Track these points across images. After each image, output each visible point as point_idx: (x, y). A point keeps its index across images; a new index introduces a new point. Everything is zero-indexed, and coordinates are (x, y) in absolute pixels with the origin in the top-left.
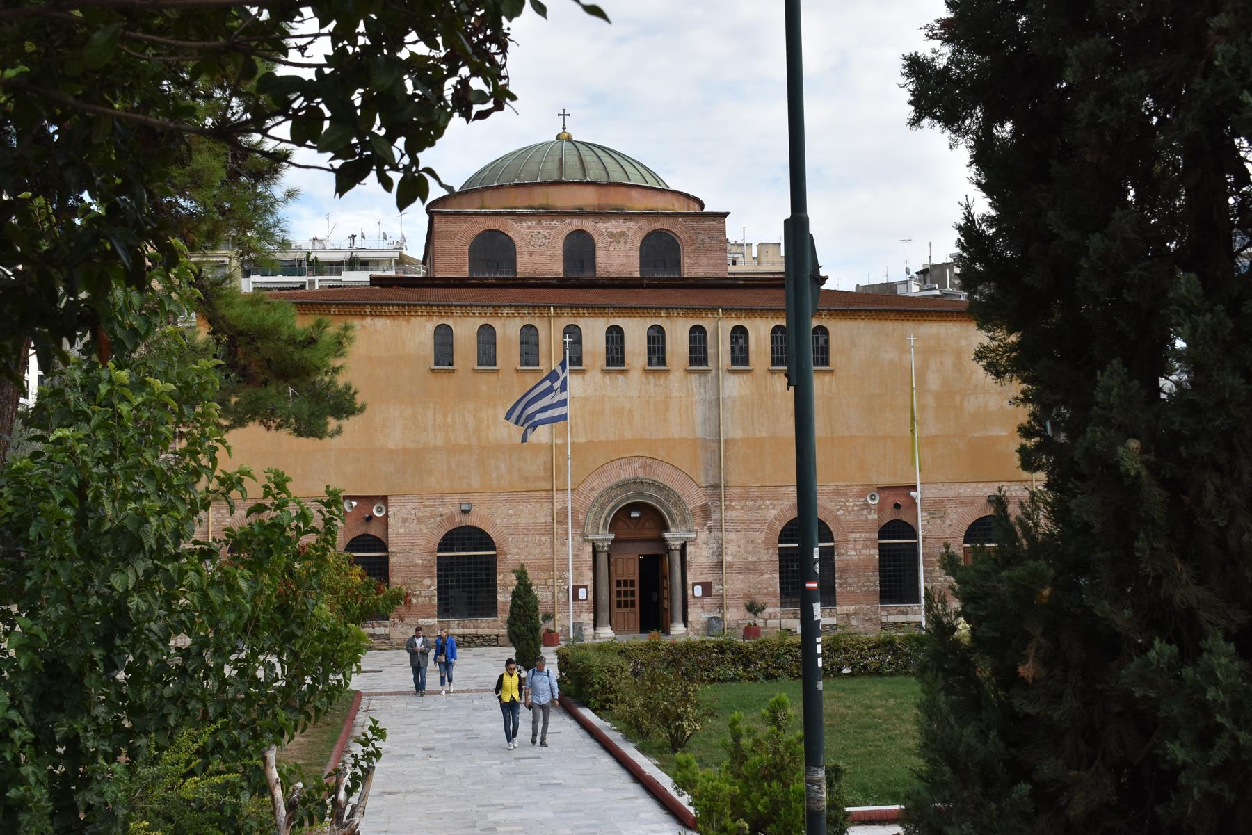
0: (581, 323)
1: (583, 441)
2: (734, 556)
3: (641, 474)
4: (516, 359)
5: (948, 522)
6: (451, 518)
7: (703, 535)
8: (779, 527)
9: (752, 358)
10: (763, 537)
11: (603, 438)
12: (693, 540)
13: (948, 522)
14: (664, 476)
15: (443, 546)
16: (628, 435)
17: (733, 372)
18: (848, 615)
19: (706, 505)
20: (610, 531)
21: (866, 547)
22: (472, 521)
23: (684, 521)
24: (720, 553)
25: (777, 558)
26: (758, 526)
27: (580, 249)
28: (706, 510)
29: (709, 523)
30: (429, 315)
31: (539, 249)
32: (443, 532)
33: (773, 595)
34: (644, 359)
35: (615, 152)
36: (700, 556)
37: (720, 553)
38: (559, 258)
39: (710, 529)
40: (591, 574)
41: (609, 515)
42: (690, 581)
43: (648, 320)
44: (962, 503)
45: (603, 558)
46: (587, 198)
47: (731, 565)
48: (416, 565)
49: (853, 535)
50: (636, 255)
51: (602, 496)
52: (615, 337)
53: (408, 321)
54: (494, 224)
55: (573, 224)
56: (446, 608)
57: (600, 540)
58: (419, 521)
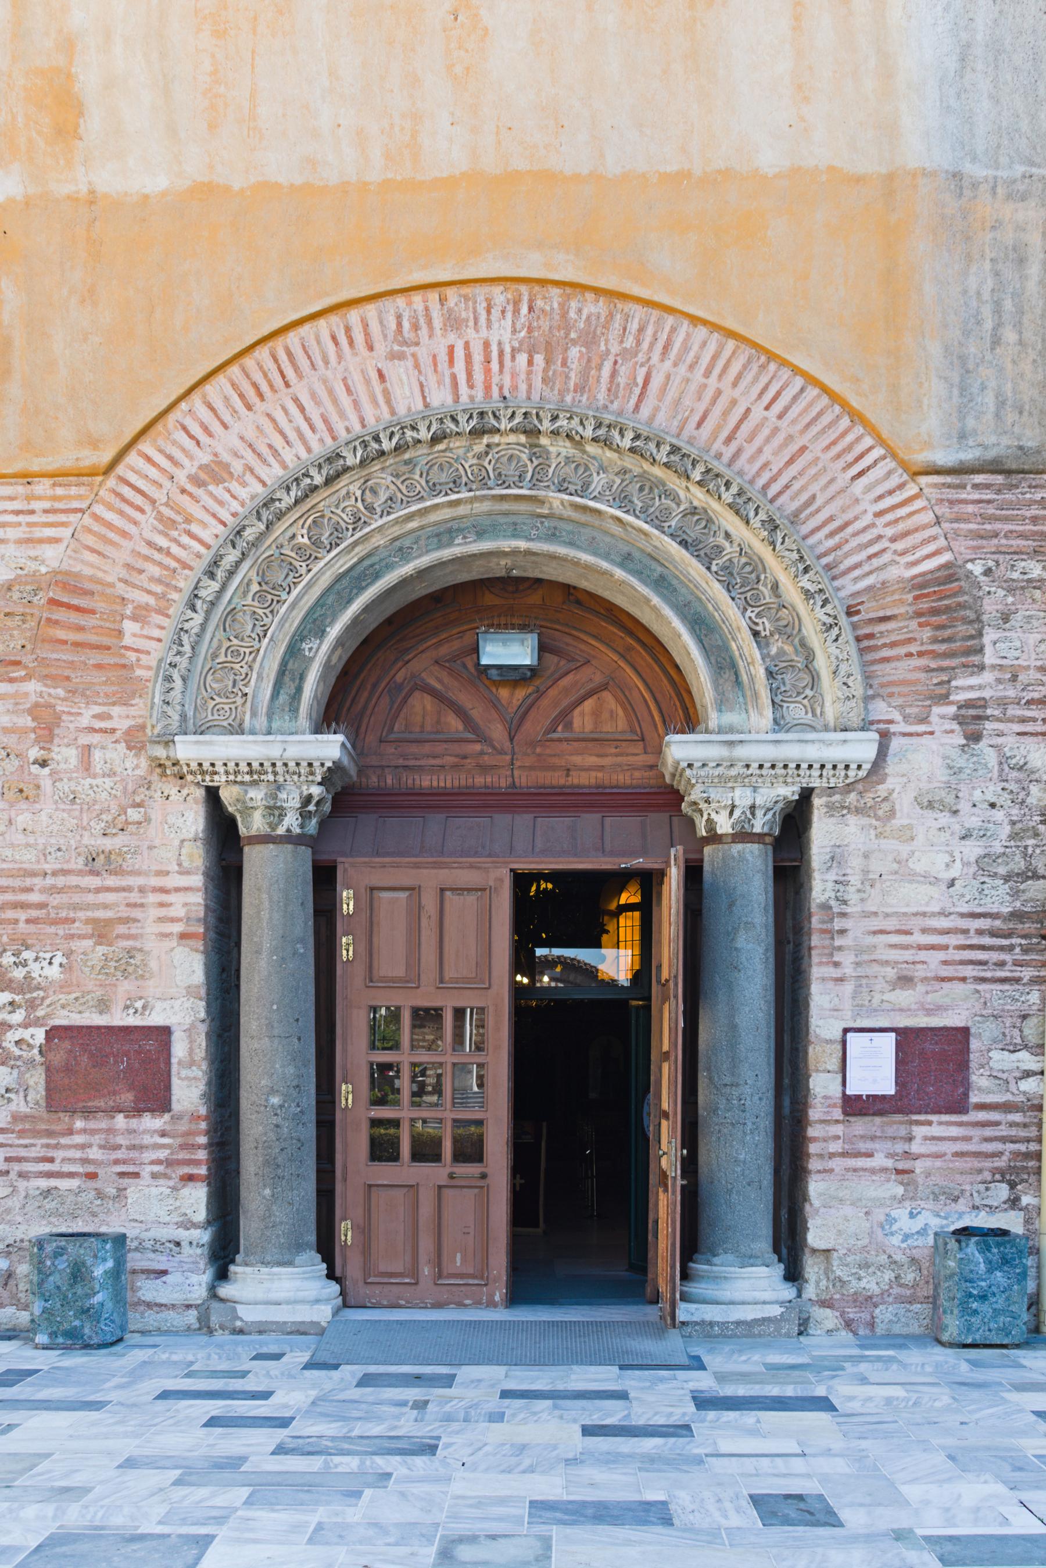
1: (157, 183)
7: (927, 756)
11: (279, 166)
20: (327, 719)
40: (190, 967)
41: (314, 625)
45: (271, 879)
51: (267, 508)
57: (256, 772)
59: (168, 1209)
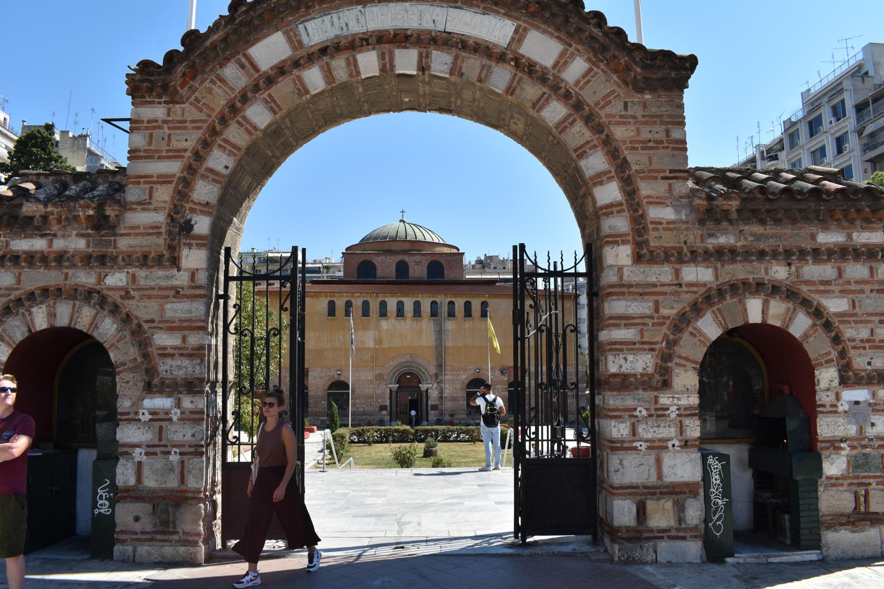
0: (387, 300)
3: (410, 359)
4: (361, 314)
6: (333, 377)
9: (456, 314)
12: (431, 388)
14: (419, 360)
15: (330, 388)
16: (405, 344)
22: (342, 378)
23: (427, 380)
24: (441, 392)
27: (402, 268)
28: (437, 375)
30: (327, 296)
31: (386, 266)
32: (330, 383)
34: (412, 314)
35: (424, 229)
36: (434, 394)
37: (441, 392)
38: (394, 271)
42: (430, 403)
45: (394, 394)
46: (407, 246)
47: (446, 398)
50: (425, 270)
52: (400, 305)
54: (367, 258)
55: (399, 258)
58: (321, 378)
59: (387, 418)
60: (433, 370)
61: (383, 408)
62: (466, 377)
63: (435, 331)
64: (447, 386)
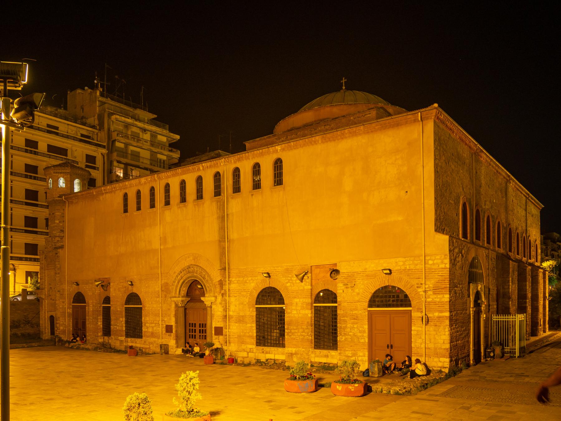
0: (170, 181)
2: (233, 312)
3: (193, 263)
5: (357, 290)
8: (256, 295)
10: (247, 300)
13: (357, 290)
17: (232, 198)
18: (292, 354)
19: (221, 280)
21: (303, 308)
25: (254, 314)
26: (245, 293)
29: (223, 292)
33: (251, 337)
36: (218, 311)
39: (223, 295)
43: (195, 173)
44: (367, 276)
48: (118, 311)
49: (297, 300)
53: (115, 193)
56: (127, 335)
60: (216, 276)
61: (169, 329)
62: (255, 285)
63: (218, 218)
64: (233, 299)
